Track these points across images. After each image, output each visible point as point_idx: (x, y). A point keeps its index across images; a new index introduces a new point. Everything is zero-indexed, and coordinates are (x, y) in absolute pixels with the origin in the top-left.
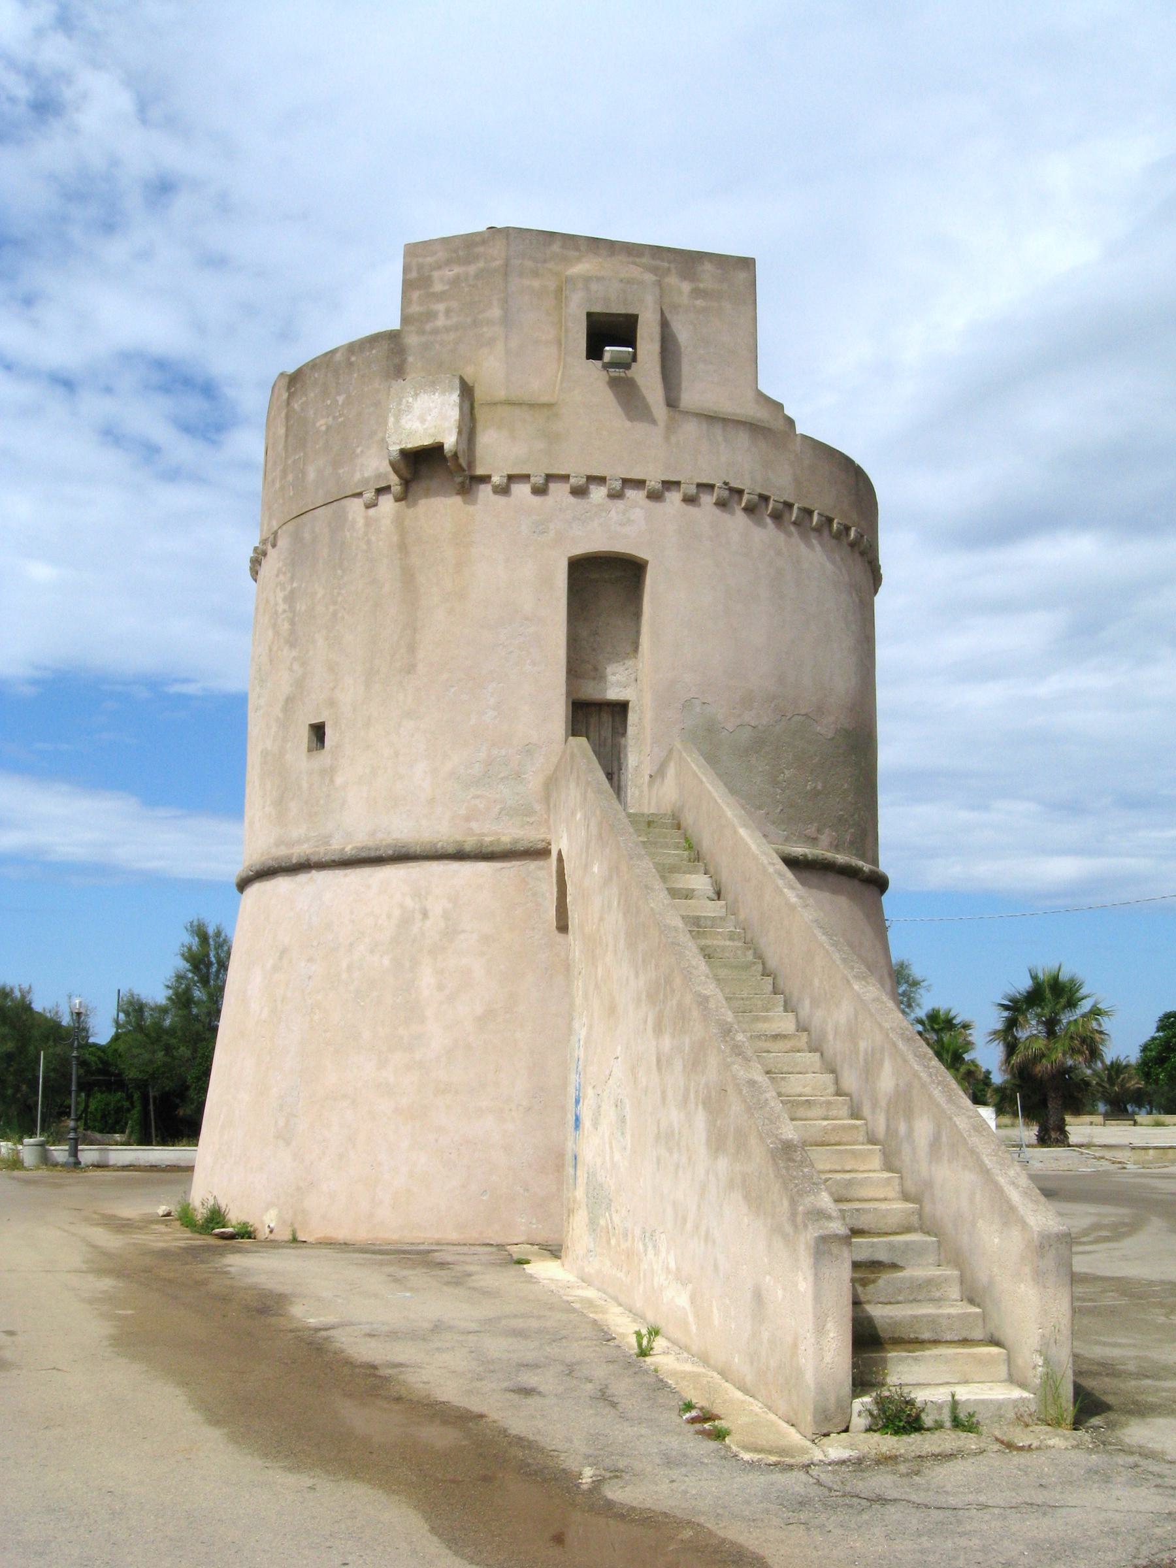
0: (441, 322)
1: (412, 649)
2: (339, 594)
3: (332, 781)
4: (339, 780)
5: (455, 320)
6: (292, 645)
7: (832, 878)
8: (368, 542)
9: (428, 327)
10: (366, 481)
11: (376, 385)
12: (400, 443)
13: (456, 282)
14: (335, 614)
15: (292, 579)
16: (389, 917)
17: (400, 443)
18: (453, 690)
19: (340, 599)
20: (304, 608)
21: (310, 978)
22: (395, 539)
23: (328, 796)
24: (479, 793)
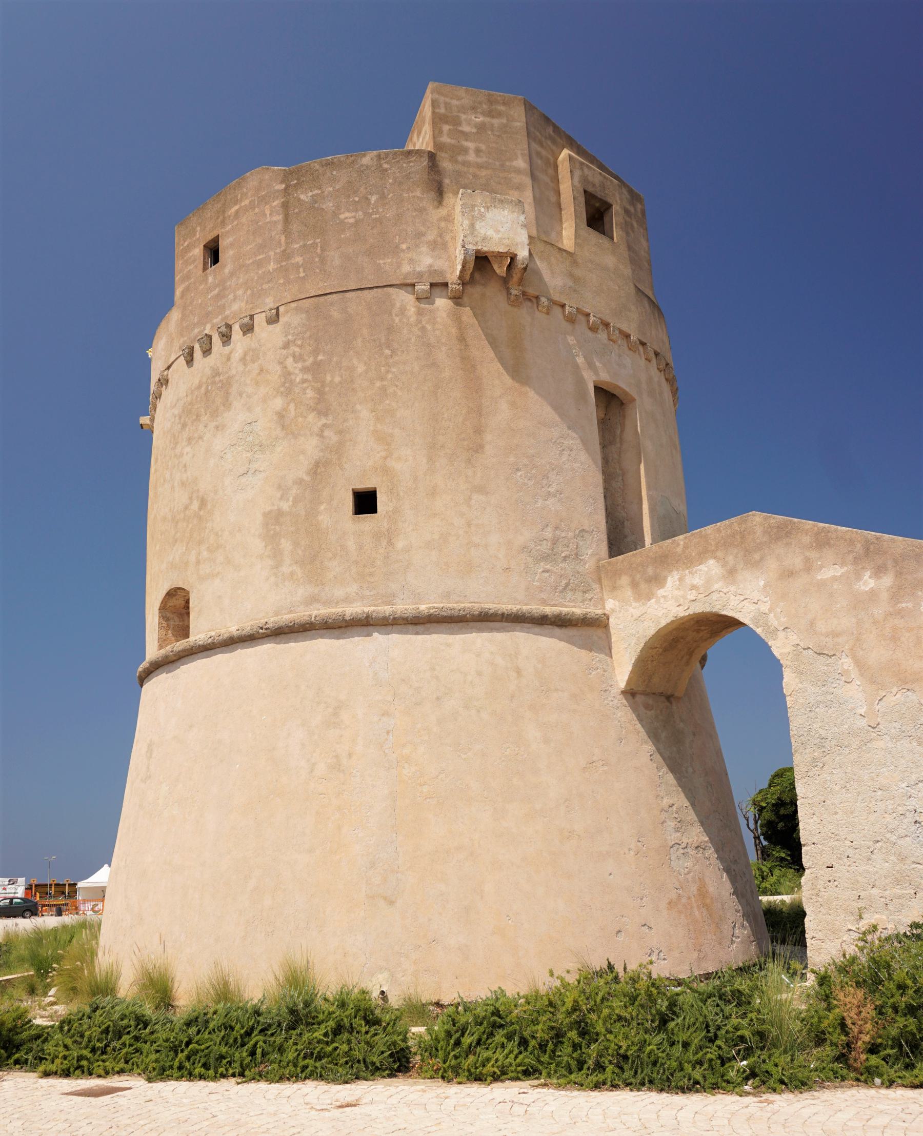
0: (471, 157)
1: (479, 431)
2: (388, 372)
3: (390, 543)
4: (400, 544)
5: (484, 159)
6: (323, 413)
7: (548, 629)
8: (423, 329)
9: (460, 158)
10: (420, 275)
11: (418, 193)
12: (476, 244)
13: (482, 128)
14: (383, 389)
15: (316, 352)
16: (479, 674)
17: (476, 244)
18: (519, 474)
19: (390, 376)
20: (337, 379)
21: (388, 732)
22: (454, 331)
23: (387, 557)
24: (548, 567)
